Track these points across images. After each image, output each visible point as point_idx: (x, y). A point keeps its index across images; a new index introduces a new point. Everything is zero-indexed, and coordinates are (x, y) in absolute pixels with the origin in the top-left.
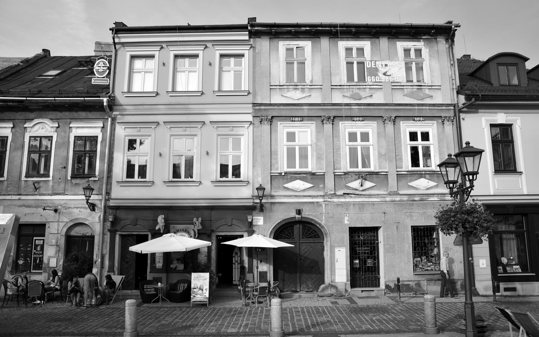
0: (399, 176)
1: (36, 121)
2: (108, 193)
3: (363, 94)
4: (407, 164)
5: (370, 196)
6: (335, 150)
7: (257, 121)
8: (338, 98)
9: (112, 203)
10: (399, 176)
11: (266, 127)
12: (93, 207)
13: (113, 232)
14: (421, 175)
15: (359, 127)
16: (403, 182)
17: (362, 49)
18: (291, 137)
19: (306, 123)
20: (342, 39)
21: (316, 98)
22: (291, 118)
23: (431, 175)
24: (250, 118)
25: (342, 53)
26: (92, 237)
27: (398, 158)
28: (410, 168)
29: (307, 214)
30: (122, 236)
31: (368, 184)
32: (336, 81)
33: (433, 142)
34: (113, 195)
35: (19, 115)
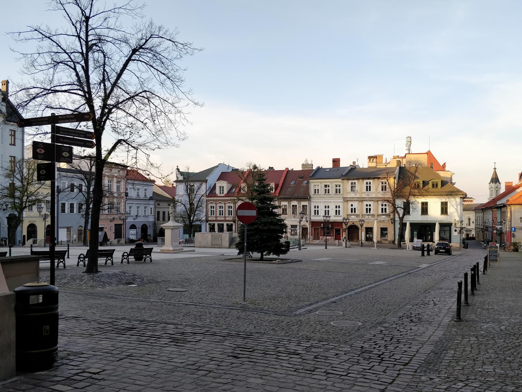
0: (378, 215)
1: (293, 201)
2: (310, 218)
3: (370, 194)
4: (380, 212)
5: (370, 220)
6: (362, 209)
7: (344, 201)
8: (364, 196)
9: (311, 221)
10: (378, 215)
11: (346, 203)
12: (307, 221)
13: (312, 227)
14: (383, 215)
15: (368, 203)
16: (379, 217)
17: (370, 182)
18: (352, 205)
19: (355, 202)
20: (365, 180)
21: (358, 196)
22: (352, 201)
23: (386, 215)
24: (342, 201)
25: (365, 183)
26: (307, 228)
27: (377, 211)
28: (381, 213)
29: (355, 224)
30: (314, 228)
31: (370, 217)
32: (363, 191)
33: (387, 208)
34: (312, 219)
35: (289, 200)
